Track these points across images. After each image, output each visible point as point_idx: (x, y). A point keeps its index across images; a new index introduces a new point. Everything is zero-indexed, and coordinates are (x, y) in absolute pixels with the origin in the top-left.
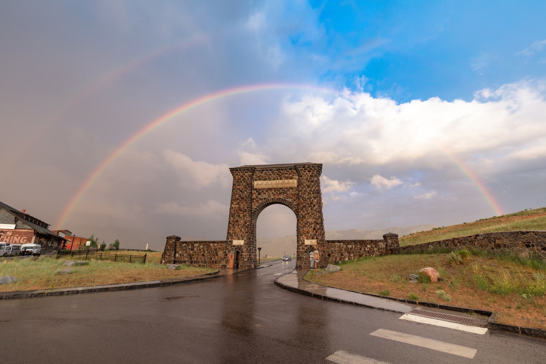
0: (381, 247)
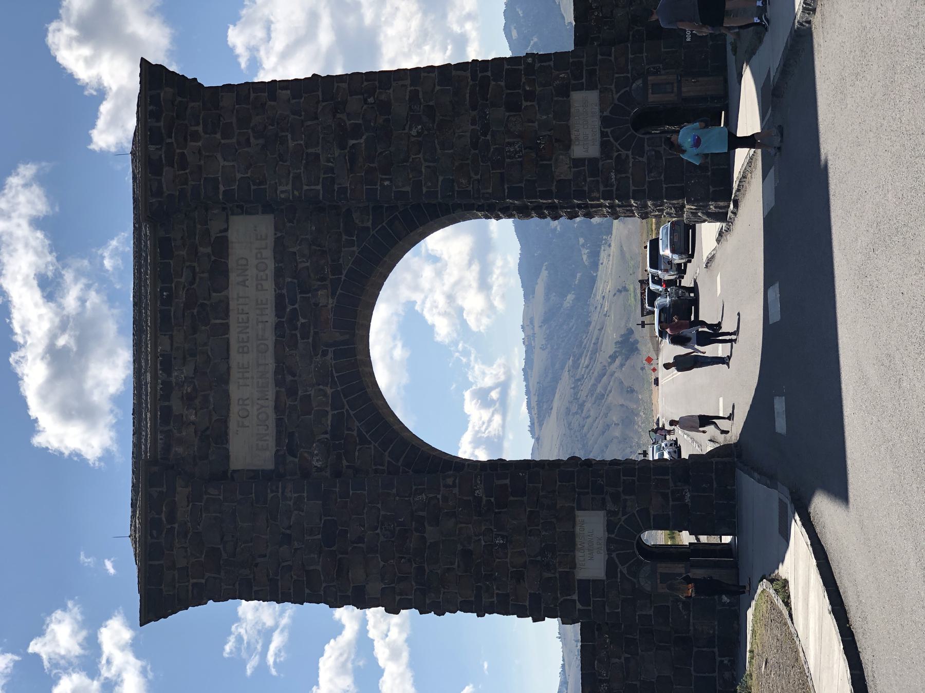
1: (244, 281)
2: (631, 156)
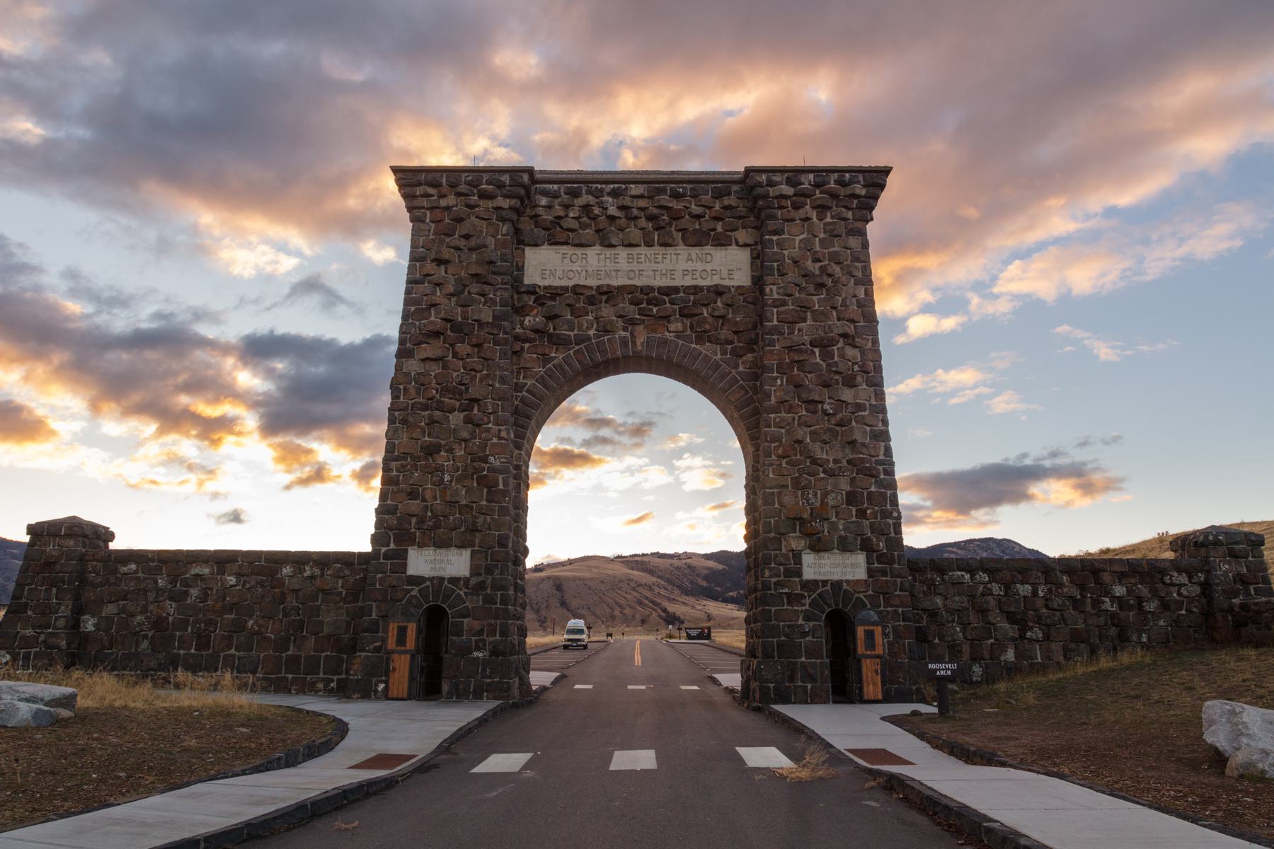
0: (1179, 594)
1: (691, 260)
2: (804, 608)
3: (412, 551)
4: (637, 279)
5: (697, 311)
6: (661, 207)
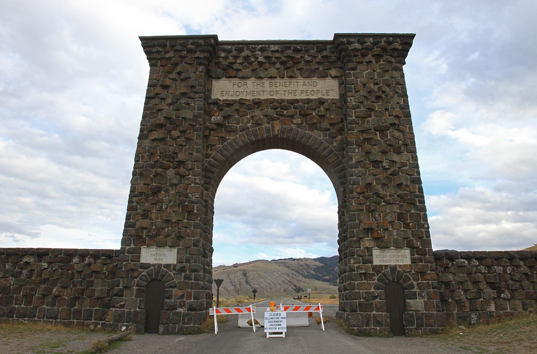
2: (374, 282)
3: (144, 249)
4: (275, 95)
5: (310, 112)
6: (288, 57)
